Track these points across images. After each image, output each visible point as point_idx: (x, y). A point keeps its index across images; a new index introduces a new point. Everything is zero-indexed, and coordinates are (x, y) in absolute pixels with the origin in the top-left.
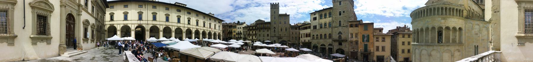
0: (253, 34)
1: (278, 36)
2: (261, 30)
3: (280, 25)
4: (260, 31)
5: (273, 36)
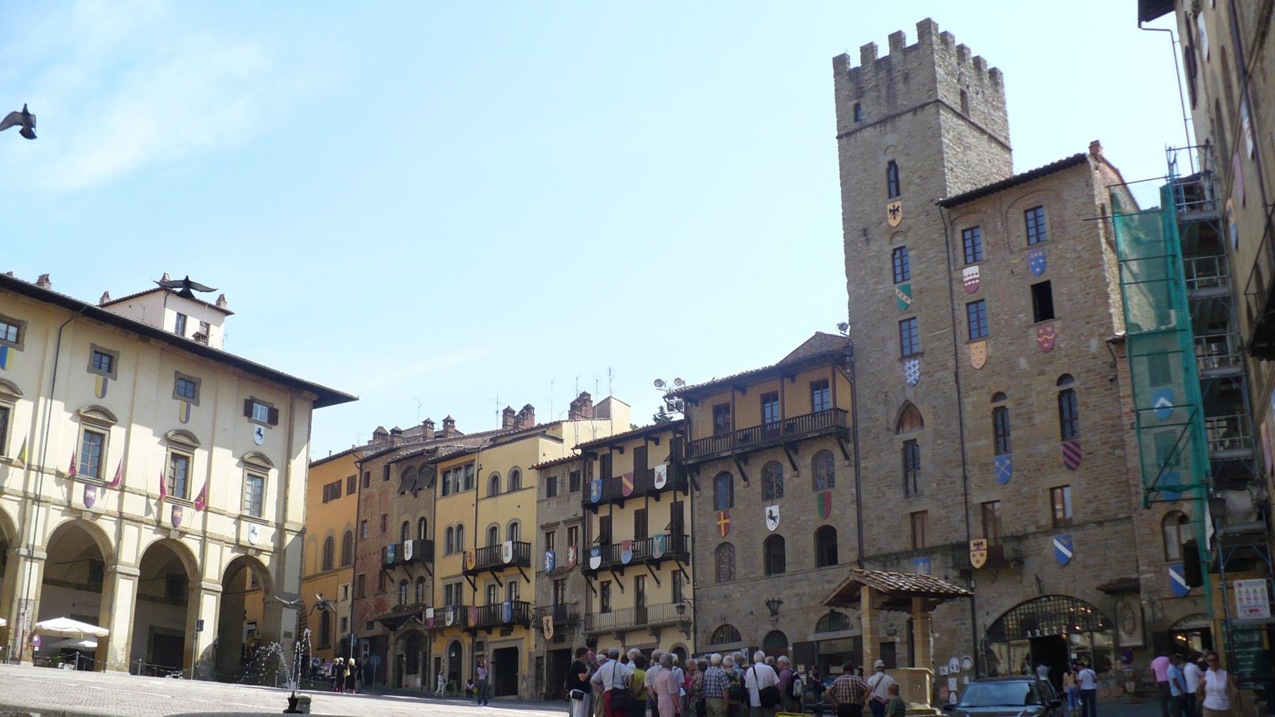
3: (977, 354)
4: (724, 501)
5: (896, 547)
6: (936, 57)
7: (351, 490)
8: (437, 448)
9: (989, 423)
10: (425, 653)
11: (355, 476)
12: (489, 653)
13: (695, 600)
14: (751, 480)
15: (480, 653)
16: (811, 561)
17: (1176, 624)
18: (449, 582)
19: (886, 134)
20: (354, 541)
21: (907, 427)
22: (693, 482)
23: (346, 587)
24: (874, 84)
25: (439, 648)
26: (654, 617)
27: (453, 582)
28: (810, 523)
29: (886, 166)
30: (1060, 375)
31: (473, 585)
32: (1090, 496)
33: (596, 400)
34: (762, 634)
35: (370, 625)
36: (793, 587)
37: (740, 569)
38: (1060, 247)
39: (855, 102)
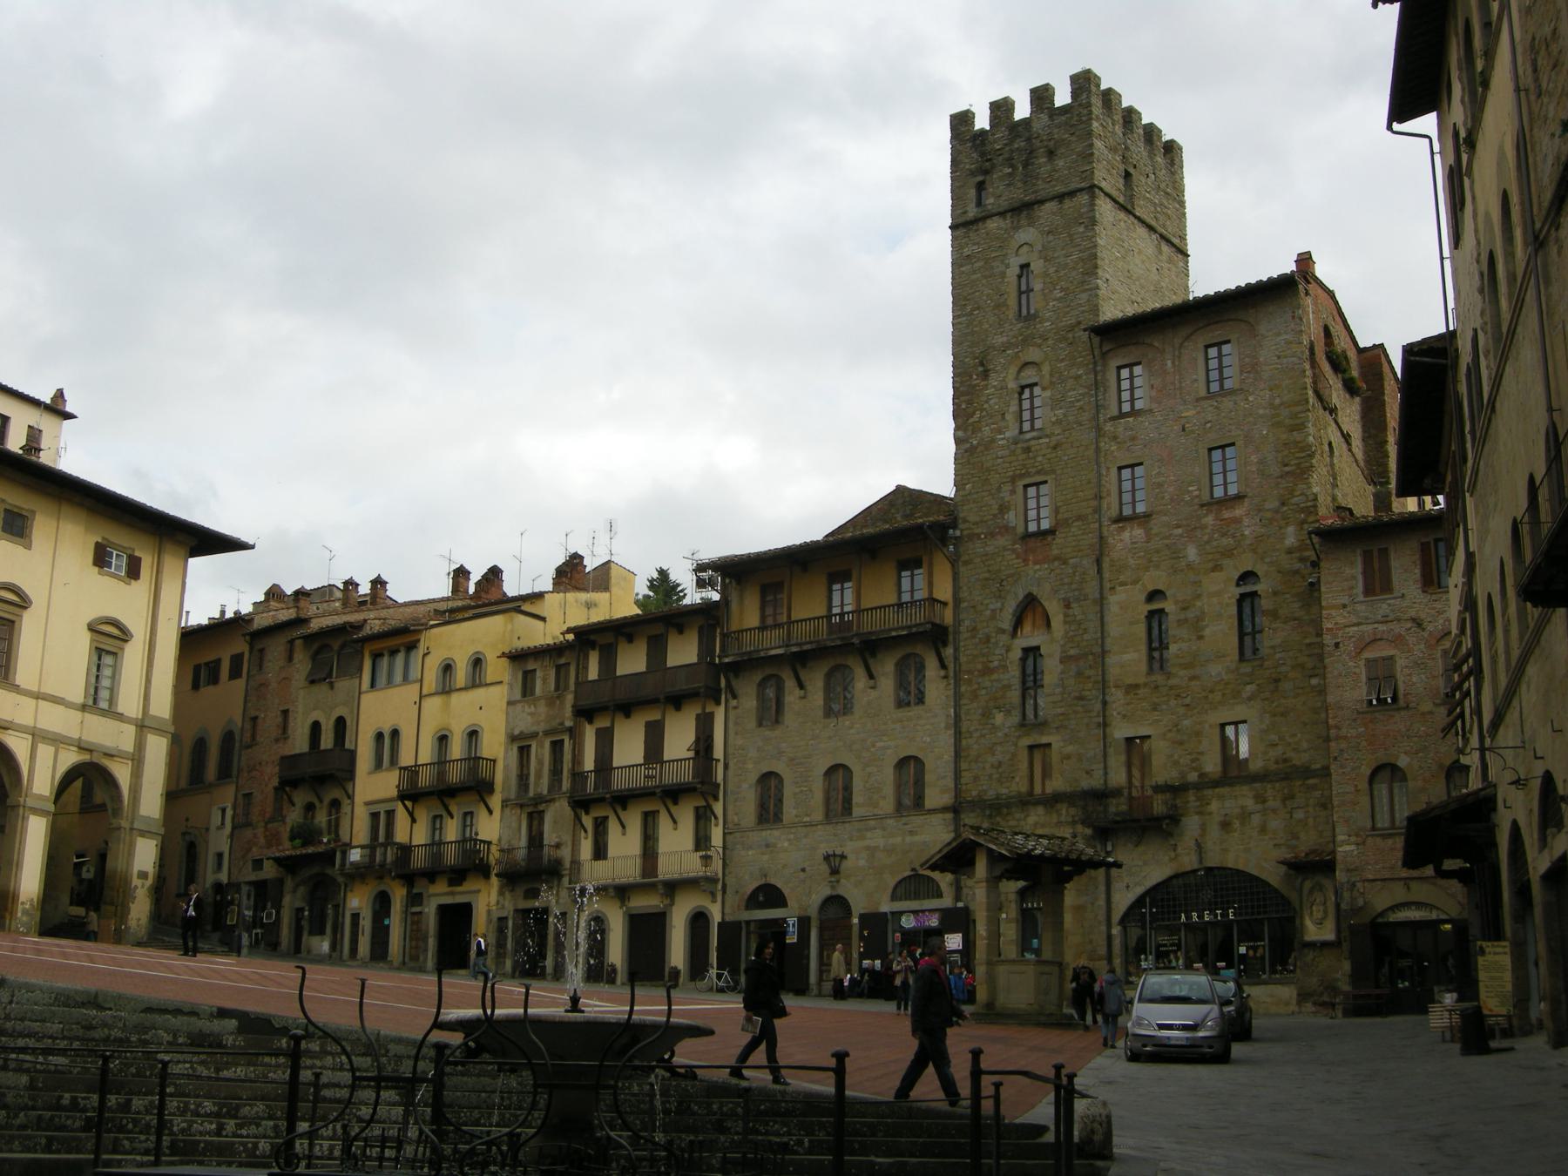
1: (1095, 782)
2: (792, 695)
4: (772, 713)
6: (1095, 124)
7: (235, 673)
8: (365, 621)
9: (1141, 629)
10: (336, 907)
11: (242, 655)
12: (430, 910)
13: (724, 848)
14: (809, 688)
15: (417, 909)
16: (888, 805)
17: (1382, 914)
18: (375, 808)
19: (1019, 228)
20: (237, 745)
21: (1027, 628)
22: (729, 685)
23: (224, 810)
24: (1006, 156)
25: (358, 901)
26: (667, 868)
27: (382, 808)
28: (889, 751)
29: (1017, 270)
30: (1242, 571)
31: (411, 814)
32: (1274, 737)
33: (590, 564)
34: (816, 899)
35: (258, 864)
37: (789, 811)
38: (1251, 399)
39: (980, 178)
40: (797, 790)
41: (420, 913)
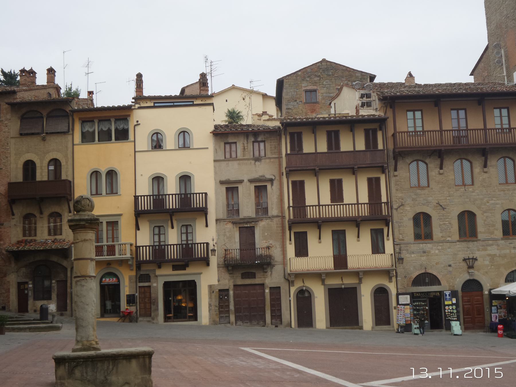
0: (337, 211)
15: (146, 284)
26: (352, 263)
28: (498, 206)
36: (486, 250)
37: (437, 233)
40: (441, 223)
41: (149, 287)
